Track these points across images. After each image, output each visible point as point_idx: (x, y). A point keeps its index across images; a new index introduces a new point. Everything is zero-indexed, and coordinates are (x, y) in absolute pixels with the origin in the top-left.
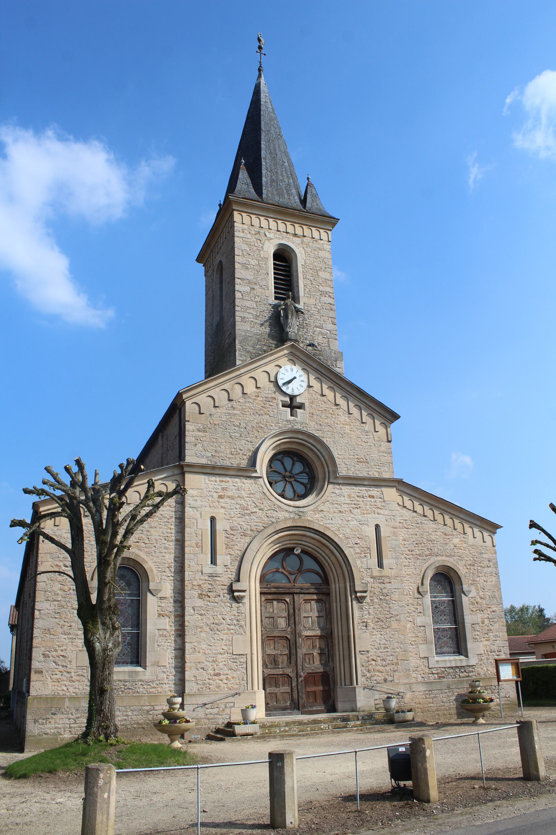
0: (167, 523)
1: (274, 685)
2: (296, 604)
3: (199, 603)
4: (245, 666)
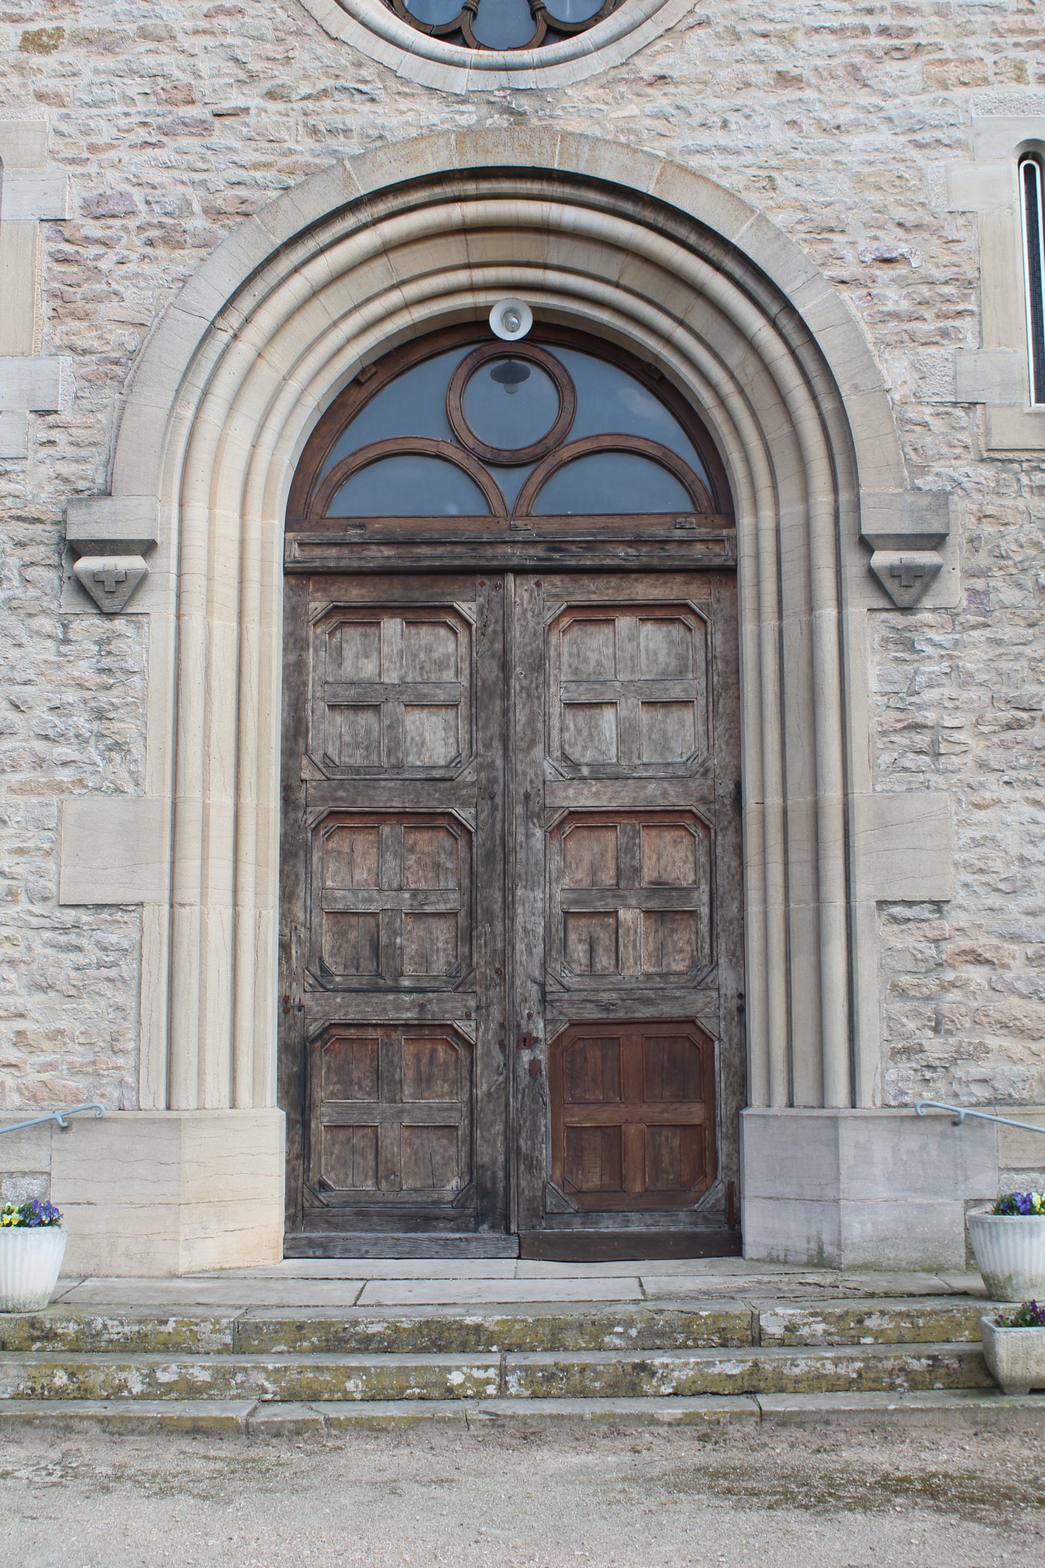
1: (368, 1083)
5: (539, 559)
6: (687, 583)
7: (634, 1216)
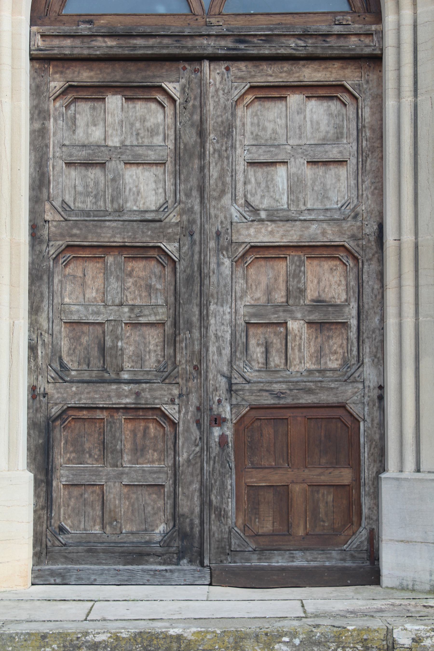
1: (96, 452)
5: (229, 49)
6: (343, 68)
7: (298, 554)
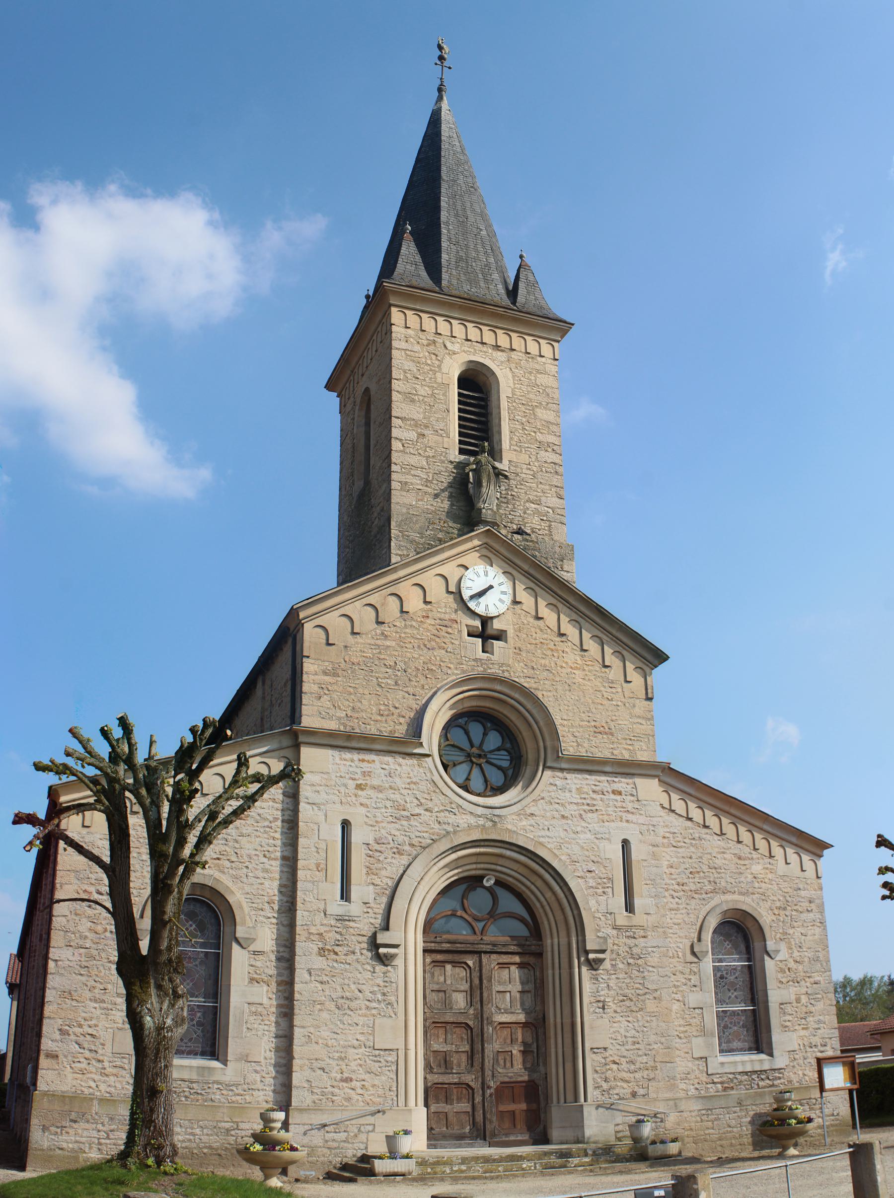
0: (268, 829)
1: (444, 1100)
2: (484, 971)
3: (319, 963)
4: (394, 1068)
